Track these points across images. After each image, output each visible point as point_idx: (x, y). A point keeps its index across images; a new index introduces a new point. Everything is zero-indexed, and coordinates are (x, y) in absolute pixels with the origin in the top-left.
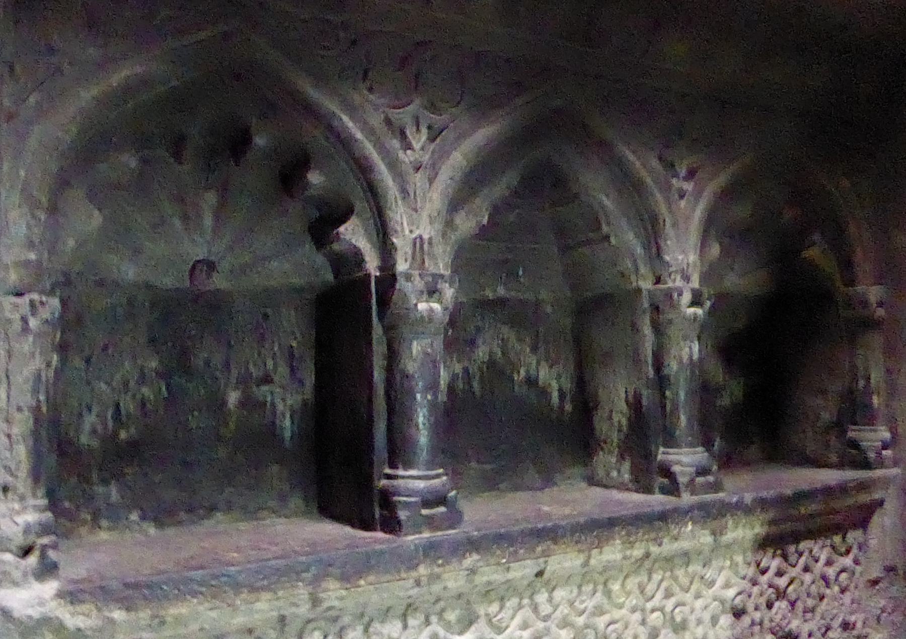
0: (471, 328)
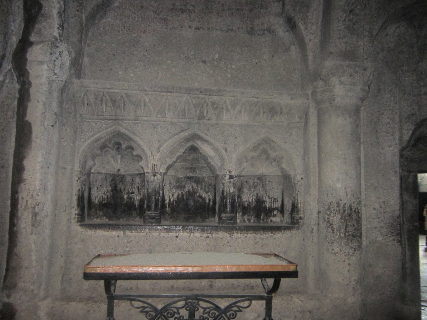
0: (184, 183)
